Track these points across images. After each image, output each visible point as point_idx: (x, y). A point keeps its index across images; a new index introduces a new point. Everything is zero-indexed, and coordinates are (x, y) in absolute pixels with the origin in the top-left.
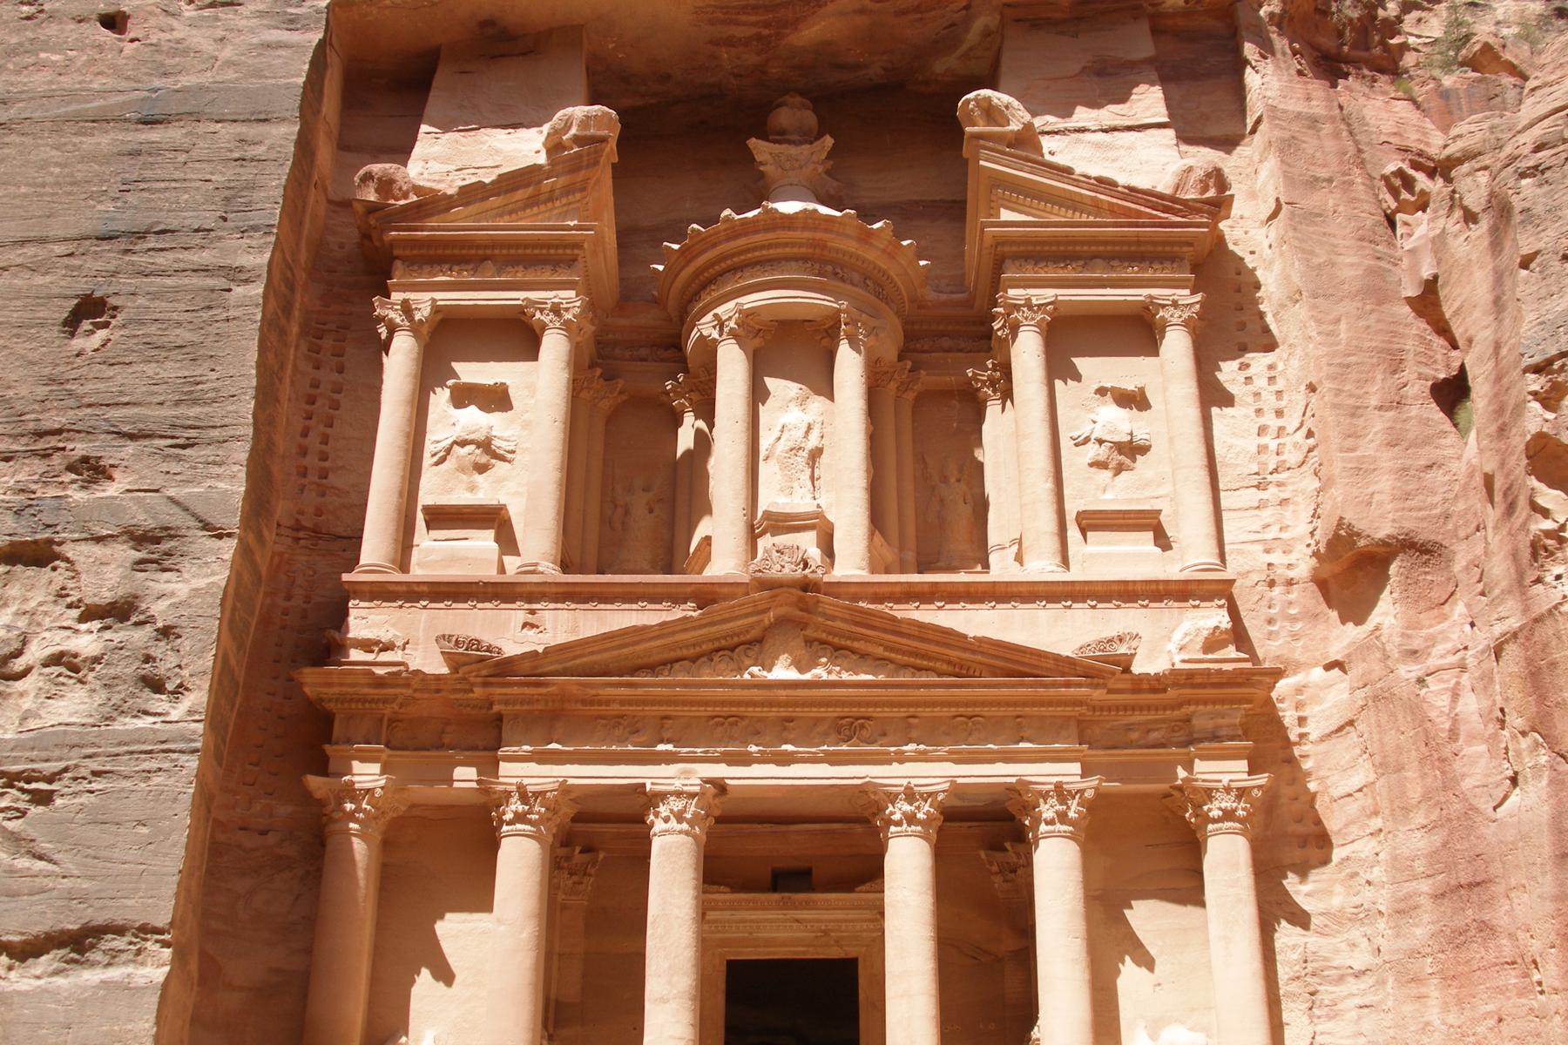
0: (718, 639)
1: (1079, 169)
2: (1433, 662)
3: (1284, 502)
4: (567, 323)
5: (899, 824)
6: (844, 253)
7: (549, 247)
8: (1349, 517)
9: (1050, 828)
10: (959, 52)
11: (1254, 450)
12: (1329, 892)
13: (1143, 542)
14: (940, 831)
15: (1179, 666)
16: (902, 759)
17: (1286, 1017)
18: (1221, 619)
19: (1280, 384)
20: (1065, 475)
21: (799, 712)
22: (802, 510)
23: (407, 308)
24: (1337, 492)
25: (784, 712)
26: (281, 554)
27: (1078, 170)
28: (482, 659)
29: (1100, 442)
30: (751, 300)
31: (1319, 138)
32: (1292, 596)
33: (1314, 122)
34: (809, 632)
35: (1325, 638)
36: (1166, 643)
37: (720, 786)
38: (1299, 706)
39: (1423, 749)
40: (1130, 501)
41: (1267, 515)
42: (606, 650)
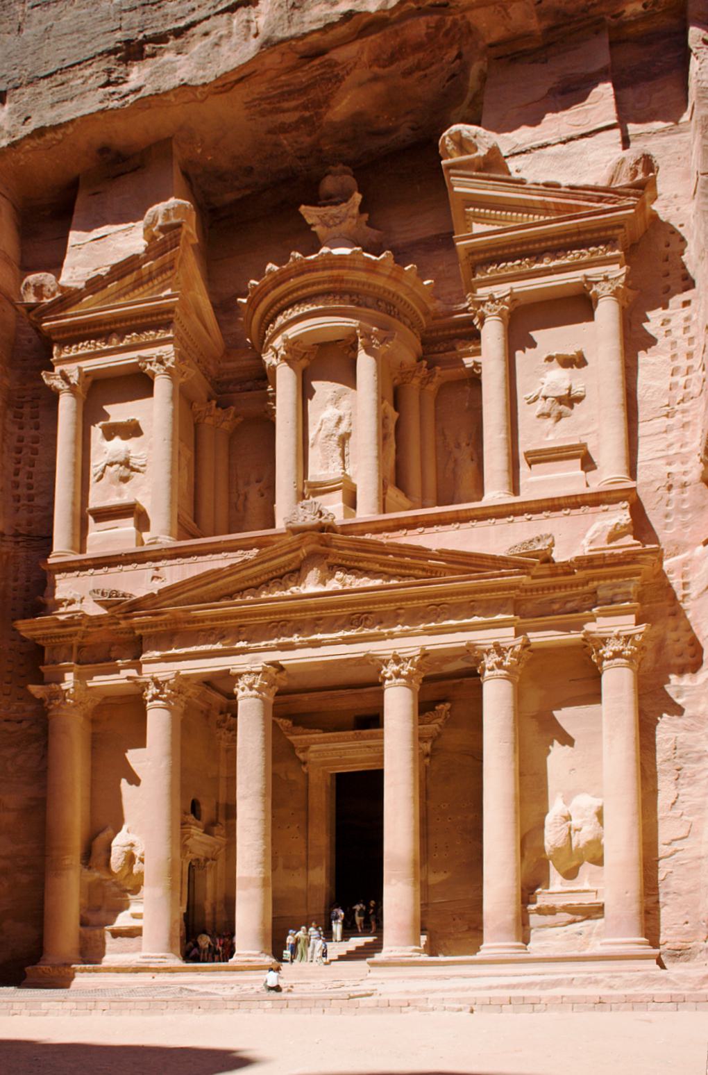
0: (271, 572)
4: (169, 370)
5: (390, 679)
6: (358, 283)
7: (152, 315)
9: (492, 673)
13: (572, 469)
16: (392, 636)
17: (660, 785)
20: (520, 427)
21: (325, 613)
22: (332, 477)
25: (315, 614)
30: (292, 332)
34: (330, 560)
42: (197, 587)
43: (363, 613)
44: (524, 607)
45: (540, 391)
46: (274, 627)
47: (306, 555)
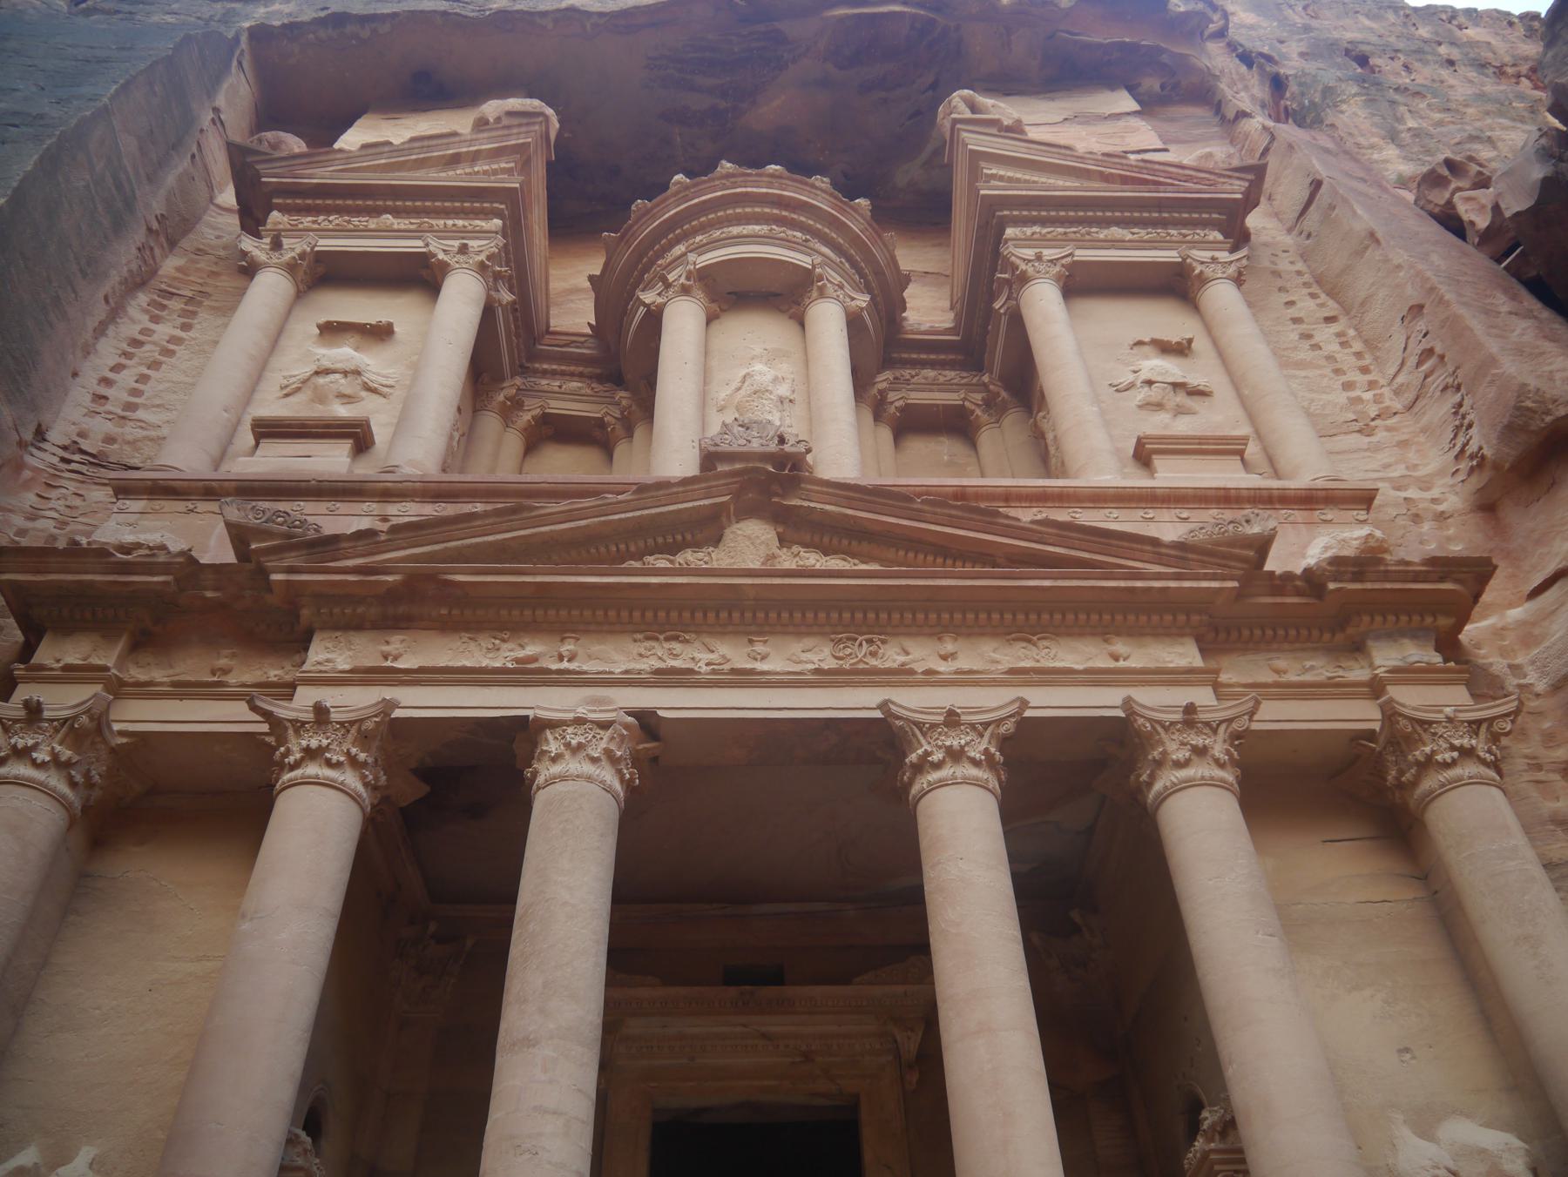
1: (1081, 147)
3: (1403, 444)
10: (924, 156)
23: (277, 245)
26: (36, 470)
28: (289, 536)
29: (1150, 383)
32: (1451, 532)
33: (1327, 151)
37: (647, 722)
41: (1384, 457)
43: (862, 634)
46: (648, 638)
47: (733, 518)
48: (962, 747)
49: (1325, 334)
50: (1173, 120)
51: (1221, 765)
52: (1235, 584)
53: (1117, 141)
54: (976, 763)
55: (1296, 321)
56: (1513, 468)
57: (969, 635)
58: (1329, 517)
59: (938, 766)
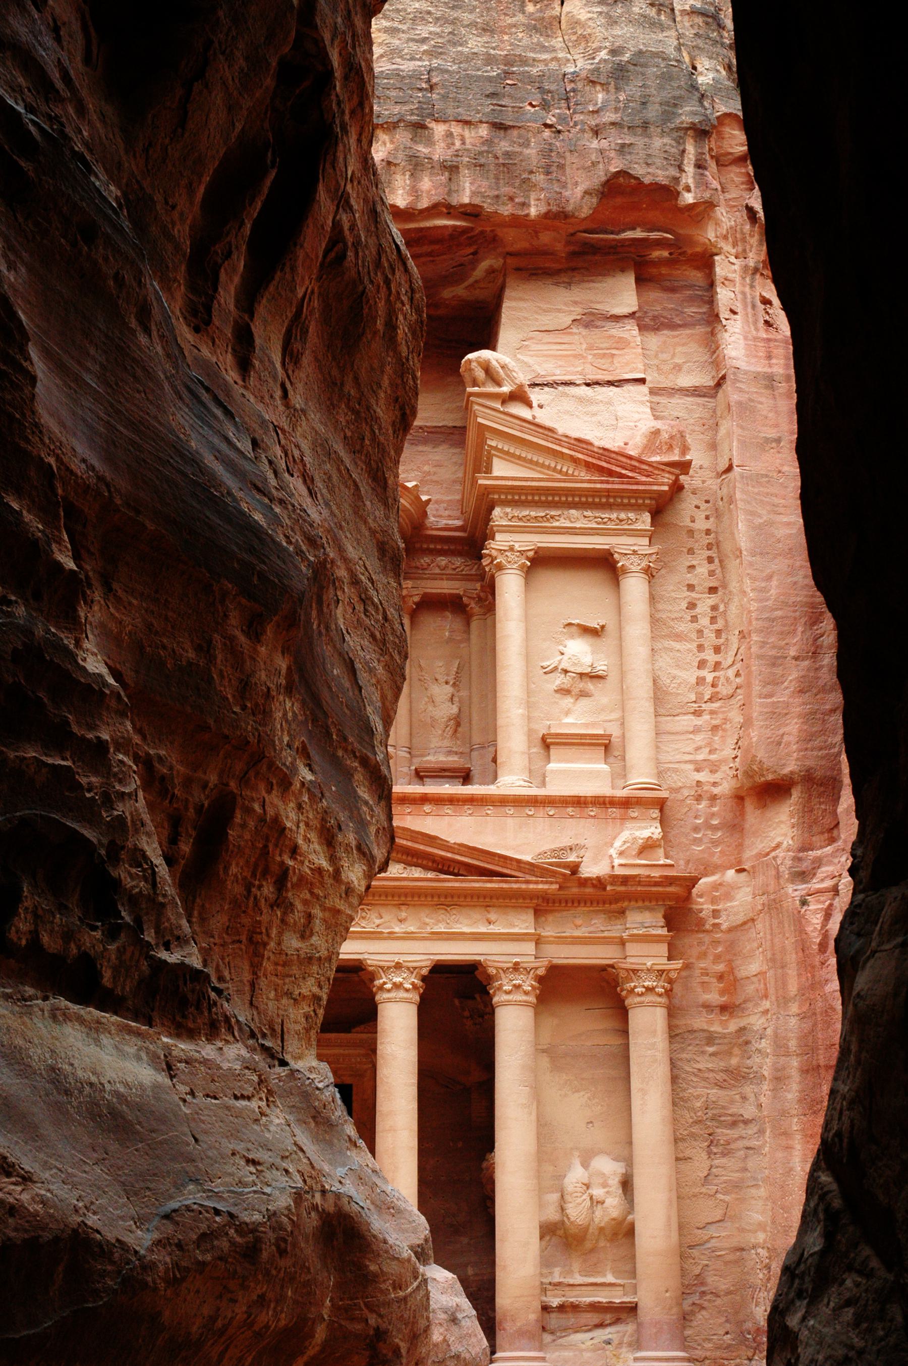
2: (815, 885)
3: (715, 728)
8: (761, 754)
10: (466, 284)
11: (693, 680)
12: (729, 1053)
14: (422, 997)
15: (619, 871)
18: (653, 831)
19: (720, 624)
24: (754, 734)
27: (561, 431)
29: (566, 672)
31: (774, 398)
33: (770, 381)
35: (741, 845)
36: (609, 851)
38: (714, 901)
39: (800, 954)
40: (586, 725)
41: (699, 738)
44: (543, 919)
45: (560, 662)
48: (401, 984)
49: (705, 604)
50: (673, 290)
51: (526, 993)
52: (556, 886)
53: (604, 363)
54: (407, 990)
55: (691, 587)
56: (751, 789)
57: (414, 905)
58: (635, 815)
59: (389, 991)
